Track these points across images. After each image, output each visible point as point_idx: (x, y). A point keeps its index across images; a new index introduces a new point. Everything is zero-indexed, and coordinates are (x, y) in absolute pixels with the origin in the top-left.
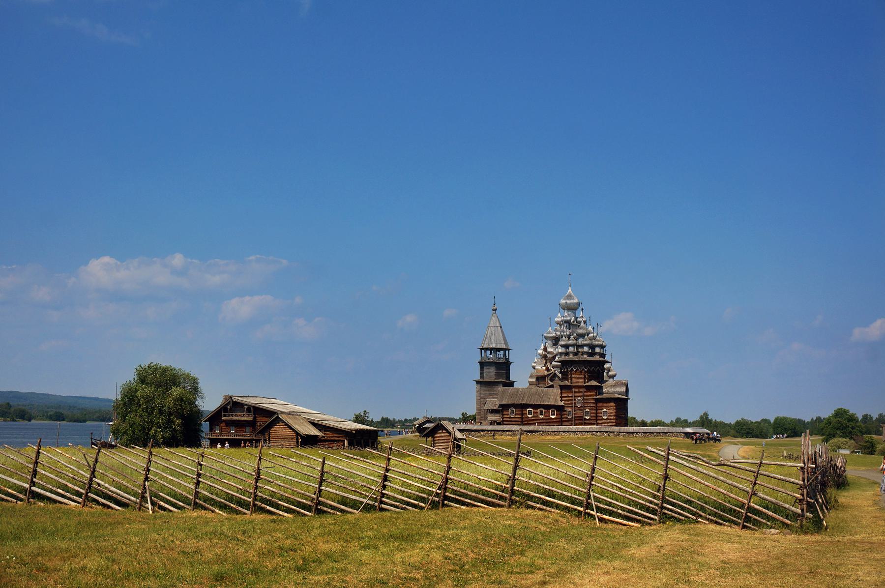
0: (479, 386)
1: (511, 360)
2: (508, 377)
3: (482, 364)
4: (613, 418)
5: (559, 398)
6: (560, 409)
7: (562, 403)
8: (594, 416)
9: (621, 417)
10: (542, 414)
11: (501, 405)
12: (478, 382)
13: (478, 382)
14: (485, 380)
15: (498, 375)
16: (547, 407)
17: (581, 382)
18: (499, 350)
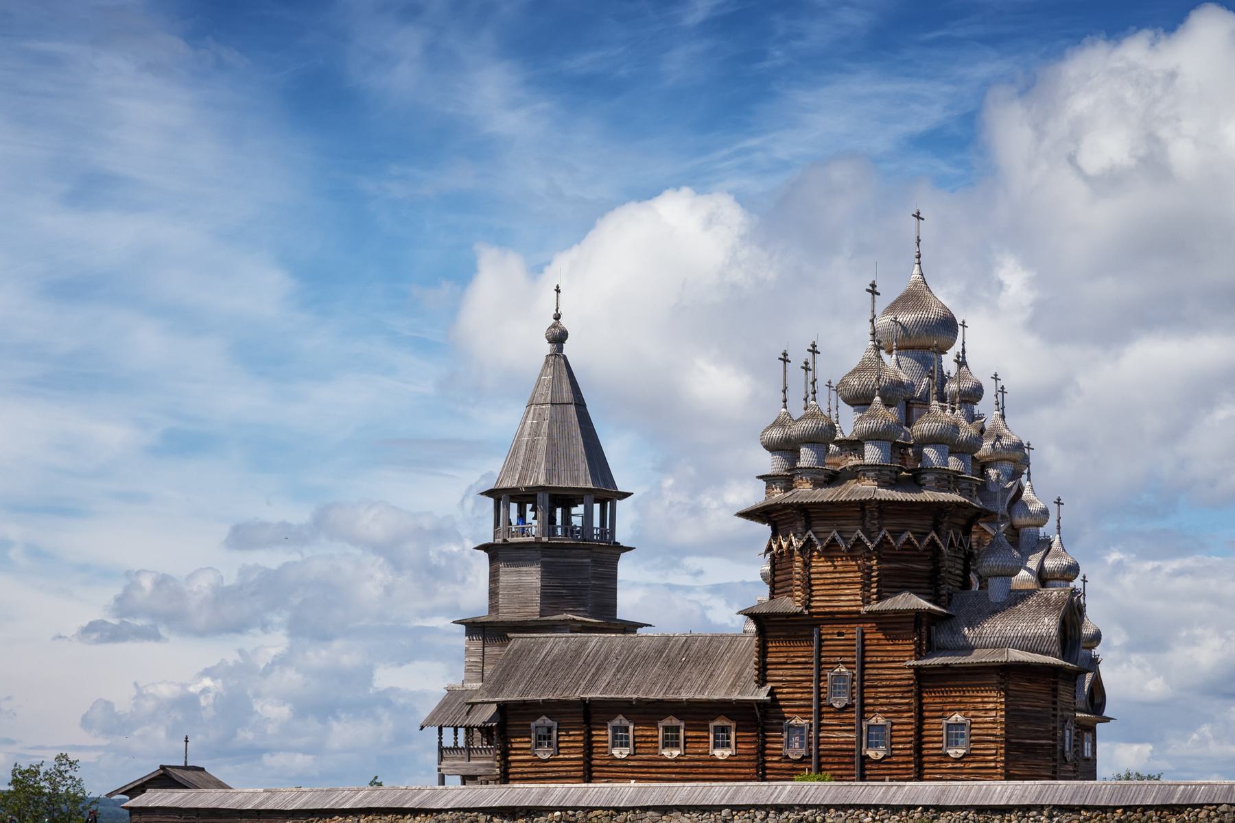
0: (477, 643)
1: (621, 537)
2: (609, 606)
3: (497, 552)
4: (994, 754)
5: (751, 671)
6: (757, 720)
7: (763, 695)
8: (905, 747)
9: (1030, 750)
10: (670, 743)
11: (503, 708)
12: (475, 628)
13: (475, 628)
14: (505, 615)
15: (550, 598)
16: (698, 714)
17: (849, 599)
18: (565, 499)
